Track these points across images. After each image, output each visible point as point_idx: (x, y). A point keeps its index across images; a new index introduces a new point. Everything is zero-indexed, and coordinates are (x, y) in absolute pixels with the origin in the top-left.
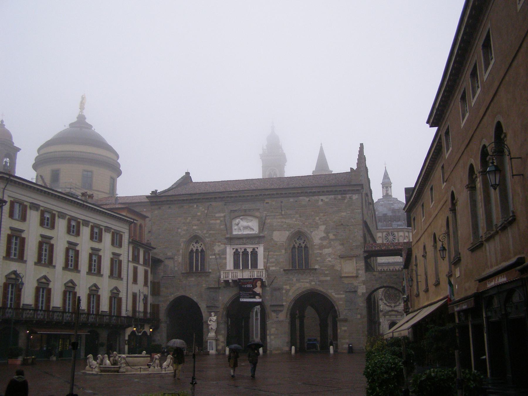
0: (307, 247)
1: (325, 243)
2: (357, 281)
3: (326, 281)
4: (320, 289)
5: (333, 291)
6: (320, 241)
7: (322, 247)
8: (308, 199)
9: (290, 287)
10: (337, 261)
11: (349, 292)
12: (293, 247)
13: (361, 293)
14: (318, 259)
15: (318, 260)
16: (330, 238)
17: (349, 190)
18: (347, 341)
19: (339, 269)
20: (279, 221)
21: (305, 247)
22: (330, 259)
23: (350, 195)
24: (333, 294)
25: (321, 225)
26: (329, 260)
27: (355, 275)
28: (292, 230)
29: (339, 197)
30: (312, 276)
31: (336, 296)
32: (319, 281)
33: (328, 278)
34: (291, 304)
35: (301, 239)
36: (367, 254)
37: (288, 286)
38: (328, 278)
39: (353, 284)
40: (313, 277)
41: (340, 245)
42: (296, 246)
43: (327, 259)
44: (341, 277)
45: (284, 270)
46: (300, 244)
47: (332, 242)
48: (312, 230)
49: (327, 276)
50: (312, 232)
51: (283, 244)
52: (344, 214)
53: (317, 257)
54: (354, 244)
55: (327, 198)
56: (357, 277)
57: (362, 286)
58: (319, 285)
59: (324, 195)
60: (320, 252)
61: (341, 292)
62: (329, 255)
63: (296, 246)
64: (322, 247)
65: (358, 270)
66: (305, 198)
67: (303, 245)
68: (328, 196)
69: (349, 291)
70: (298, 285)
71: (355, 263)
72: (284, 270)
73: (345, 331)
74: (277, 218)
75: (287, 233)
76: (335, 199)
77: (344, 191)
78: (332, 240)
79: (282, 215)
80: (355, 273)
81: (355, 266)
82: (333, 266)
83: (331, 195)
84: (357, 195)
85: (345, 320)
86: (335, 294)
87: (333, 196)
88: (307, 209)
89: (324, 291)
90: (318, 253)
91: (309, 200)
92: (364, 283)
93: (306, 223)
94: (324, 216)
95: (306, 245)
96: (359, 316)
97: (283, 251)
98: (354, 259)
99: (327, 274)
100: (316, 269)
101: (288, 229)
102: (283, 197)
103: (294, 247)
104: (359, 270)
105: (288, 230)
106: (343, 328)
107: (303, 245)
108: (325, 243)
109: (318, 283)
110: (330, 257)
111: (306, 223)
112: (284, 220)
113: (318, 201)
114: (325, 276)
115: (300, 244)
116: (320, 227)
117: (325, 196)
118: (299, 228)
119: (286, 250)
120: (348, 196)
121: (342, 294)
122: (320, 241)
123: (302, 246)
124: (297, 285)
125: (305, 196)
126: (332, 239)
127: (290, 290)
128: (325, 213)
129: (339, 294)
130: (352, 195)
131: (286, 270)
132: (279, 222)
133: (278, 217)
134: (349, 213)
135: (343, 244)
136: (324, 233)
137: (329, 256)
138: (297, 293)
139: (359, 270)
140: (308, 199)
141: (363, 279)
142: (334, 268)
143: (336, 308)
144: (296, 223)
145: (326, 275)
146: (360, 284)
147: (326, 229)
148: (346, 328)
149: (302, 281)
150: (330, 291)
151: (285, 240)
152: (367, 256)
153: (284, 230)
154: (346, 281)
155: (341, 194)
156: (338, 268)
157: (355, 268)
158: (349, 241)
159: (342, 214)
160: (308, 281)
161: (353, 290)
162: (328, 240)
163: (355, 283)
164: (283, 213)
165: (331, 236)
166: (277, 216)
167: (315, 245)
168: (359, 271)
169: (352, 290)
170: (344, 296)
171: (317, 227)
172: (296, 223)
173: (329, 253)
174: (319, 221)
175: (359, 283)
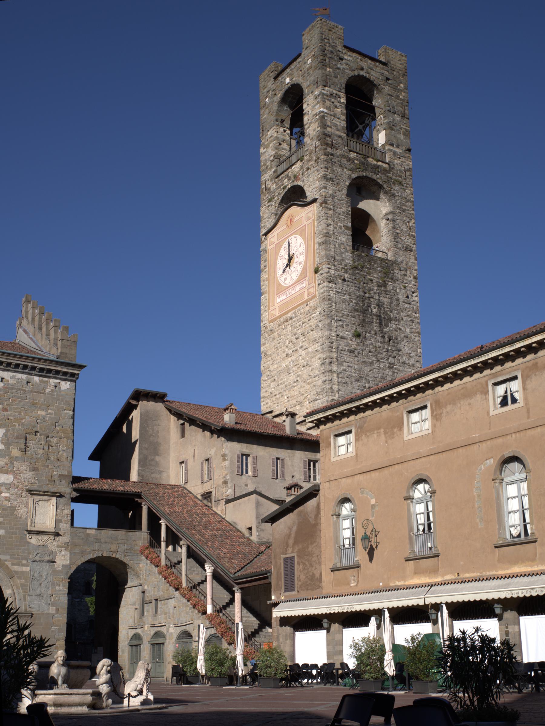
5: (7, 557)
11: (40, 561)
16: (12, 454)
22: (7, 495)
23: (57, 381)
24: (8, 564)
26: (6, 497)
27: (53, 530)
29: (37, 379)
39: (48, 547)
41: (30, 471)
43: (3, 495)
47: (15, 463)
52: (43, 413)
54: (55, 473)
57: (63, 553)
61: (24, 562)
65: (58, 521)
68: (14, 374)
76: (28, 382)
77: (50, 371)
78: (16, 459)
80: (53, 525)
83: (23, 373)
84: (69, 383)
94: (6, 410)
96: (52, 610)
98: (54, 500)
104: (62, 522)
117: (10, 373)
120: (53, 381)
121: (23, 565)
126: (17, 457)
128: (8, 405)
129: (19, 565)
130: (60, 381)
134: (51, 414)
135: (34, 469)
137: (8, 489)
139: (61, 521)
141: (68, 541)
147: (5, 435)
152: (77, 496)
154: (34, 540)
156: (21, 512)
158: (48, 466)
159: (39, 412)
161: (47, 558)
165: (15, 452)
169: (43, 559)
170: (28, 569)
173: (7, 484)
175: (58, 546)
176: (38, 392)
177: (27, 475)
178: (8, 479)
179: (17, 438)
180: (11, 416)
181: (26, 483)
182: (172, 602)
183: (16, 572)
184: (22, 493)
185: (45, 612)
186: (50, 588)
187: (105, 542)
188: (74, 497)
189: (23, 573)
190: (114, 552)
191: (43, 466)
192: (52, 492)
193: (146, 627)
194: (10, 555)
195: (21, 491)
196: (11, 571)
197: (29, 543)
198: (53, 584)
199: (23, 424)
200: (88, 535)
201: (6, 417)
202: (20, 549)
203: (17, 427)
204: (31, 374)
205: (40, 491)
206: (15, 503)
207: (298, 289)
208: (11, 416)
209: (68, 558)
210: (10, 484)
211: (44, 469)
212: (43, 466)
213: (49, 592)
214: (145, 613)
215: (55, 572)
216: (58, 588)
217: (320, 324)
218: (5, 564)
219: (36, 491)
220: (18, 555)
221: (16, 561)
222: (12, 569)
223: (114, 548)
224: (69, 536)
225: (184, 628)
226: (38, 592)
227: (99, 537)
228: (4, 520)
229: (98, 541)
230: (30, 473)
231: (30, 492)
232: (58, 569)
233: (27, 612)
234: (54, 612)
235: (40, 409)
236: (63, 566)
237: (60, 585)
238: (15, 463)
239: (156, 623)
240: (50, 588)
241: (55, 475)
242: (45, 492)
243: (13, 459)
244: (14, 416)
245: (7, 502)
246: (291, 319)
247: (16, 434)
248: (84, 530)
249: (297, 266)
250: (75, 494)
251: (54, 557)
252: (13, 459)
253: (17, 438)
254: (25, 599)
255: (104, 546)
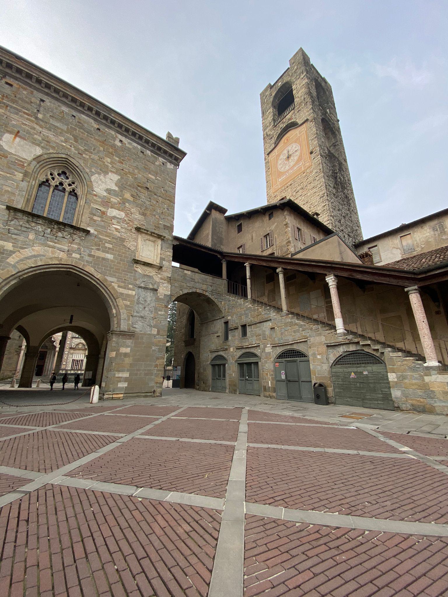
0: (76, 195)
1: (114, 200)
2: (159, 276)
3: (104, 259)
4: (90, 269)
6: (105, 194)
7: (106, 203)
8: (98, 127)
9: (13, 246)
10: (131, 235)
12: (44, 182)
13: (163, 295)
14: (95, 218)
15: (95, 221)
17: (165, 152)
18: (126, 375)
19: (133, 248)
20: (27, 123)
21: (71, 192)
22: (119, 227)
24: (116, 286)
25: (111, 171)
26: (116, 229)
28: (51, 151)
29: (149, 152)
30: (76, 241)
31: (121, 290)
32: (90, 255)
33: (110, 256)
34: (6, 285)
35: (67, 178)
36: (178, 244)
37: (11, 244)
38: (110, 256)
39: (153, 278)
40: (79, 244)
41: (140, 214)
42: (53, 183)
43: (113, 225)
44: (137, 262)
45: (9, 208)
46: (61, 184)
47: (127, 204)
48: (93, 170)
49: (108, 253)
50: (93, 174)
51: (21, 161)
52: (153, 177)
53: (95, 215)
54: (162, 223)
55: (129, 143)
56: (160, 268)
57: (165, 285)
58: (87, 261)
59: (126, 137)
60: (103, 209)
61: (130, 286)
62: (119, 220)
63: (53, 183)
64: (106, 203)
65: (162, 259)
66: (92, 121)
67: (68, 189)
69: (144, 286)
70: (38, 249)
71: (160, 245)
72: (9, 208)
73: (126, 355)
74: (21, 116)
75: (38, 151)
77: (159, 149)
78: (128, 201)
79: (37, 118)
81: (160, 253)
82: (122, 240)
83: (138, 143)
84: (173, 165)
85: (129, 334)
86: (119, 286)
87: (139, 147)
88: (92, 138)
89: (98, 276)
90: (98, 211)
91: (99, 129)
92: (170, 280)
93: (84, 155)
95: (74, 190)
96: (155, 331)
97: (20, 176)
98: (159, 242)
99: (109, 248)
100: (88, 232)
101: (42, 145)
102: (47, 94)
103: (45, 183)
105: (43, 148)
106: (123, 350)
107: (68, 189)
108: (114, 200)
109: (87, 258)
110: (120, 225)
111: (84, 155)
112: (37, 127)
113: (114, 139)
114: (103, 251)
115: (61, 184)
116: (110, 174)
118: (67, 155)
119: (26, 174)
120: (161, 159)
122: (105, 194)
123: (64, 189)
124: (36, 248)
125: (95, 120)
127: (13, 252)
131: (16, 210)
132: (23, 124)
133: (26, 116)
134: (159, 180)
135: (144, 214)
136: (116, 185)
137: (118, 222)
138: (31, 263)
140: (96, 126)
142: (124, 244)
143: (114, 311)
144: (65, 144)
145: (107, 250)
146: (163, 281)
148: (128, 350)
149: (51, 243)
150: (109, 279)
151: (30, 159)
153: (33, 143)
154: (140, 269)
155: (152, 151)
156: (130, 244)
157: (159, 256)
158: (155, 216)
159: (150, 175)
160: (66, 248)
161: (151, 286)
162: (120, 198)
163: (157, 278)
164: (40, 116)
165: (128, 196)
166: (24, 113)
167: (96, 196)
168: (164, 263)
170: (134, 293)
171: (105, 171)
172: (65, 144)
173: (118, 218)
174: (110, 166)
175: (161, 279)
176: (149, 161)
177: (138, 216)
178: (119, 215)
179: (130, 186)
180: (126, 169)
181: (136, 223)
182: (269, 324)
183: (122, 294)
184: (131, 230)
185: (149, 332)
186: (153, 313)
187: (198, 282)
188: (175, 244)
189: (128, 295)
190: (205, 291)
191: (151, 214)
192: (158, 235)
193: (232, 349)
194: (117, 278)
195: (130, 228)
196: (117, 292)
197: (136, 271)
198: (156, 309)
199: (136, 178)
200: (186, 274)
201: (122, 169)
202: (128, 275)
203: (130, 178)
204: (144, 147)
205: (148, 231)
206: (124, 236)
207: (295, 168)
208: (126, 169)
209: (170, 290)
210: (121, 219)
211: (151, 217)
212: (151, 214)
213: (152, 316)
214: (230, 338)
215: (158, 299)
216: (159, 313)
217: (316, 178)
218: (111, 285)
219: (145, 230)
220: (126, 280)
221: (123, 284)
222: (118, 291)
223: (204, 287)
224: (171, 272)
225: (289, 347)
226: (142, 315)
227: (193, 278)
228: (113, 247)
229: (193, 280)
230: (140, 216)
231: (138, 229)
232: (160, 297)
233: (131, 331)
234: (156, 333)
235: (150, 173)
236: (165, 295)
237: (161, 311)
238: (127, 204)
239: (246, 344)
240: (153, 313)
241: (161, 224)
242: (152, 233)
243: (124, 201)
244: (128, 170)
245: (117, 233)
246: (291, 185)
247: (129, 183)
248: (183, 270)
249: (295, 158)
250: (176, 243)
251: (158, 287)
252: (124, 201)
253: (130, 186)
254: (129, 319)
255: (197, 284)
